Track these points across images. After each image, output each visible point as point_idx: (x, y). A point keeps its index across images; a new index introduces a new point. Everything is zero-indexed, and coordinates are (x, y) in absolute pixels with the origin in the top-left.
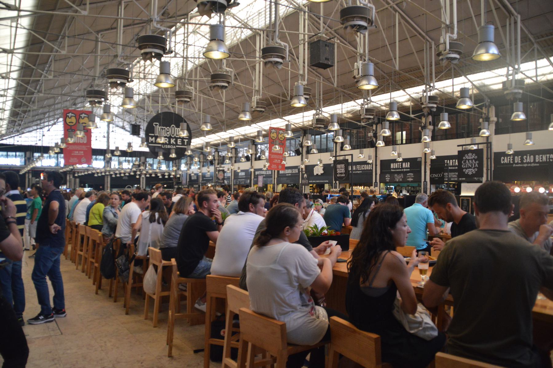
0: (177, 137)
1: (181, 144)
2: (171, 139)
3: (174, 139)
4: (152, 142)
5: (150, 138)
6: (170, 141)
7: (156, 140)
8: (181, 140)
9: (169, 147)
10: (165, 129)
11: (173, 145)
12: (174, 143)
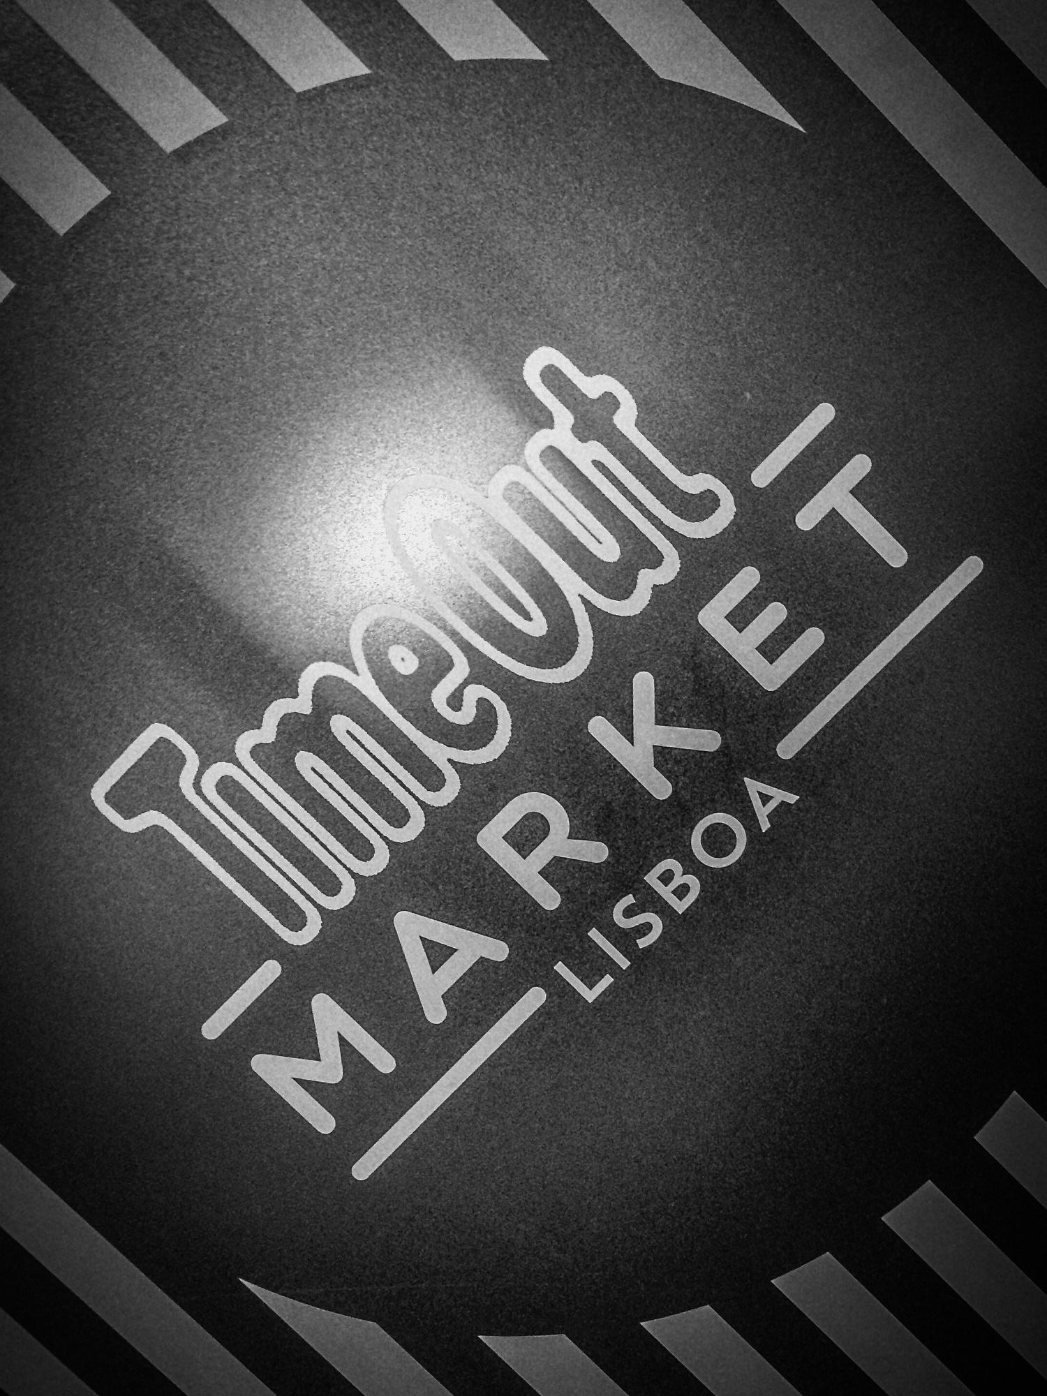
0: (635, 604)
1: (812, 640)
2: (600, 728)
3: (644, 685)
8: (747, 579)
12: (707, 740)
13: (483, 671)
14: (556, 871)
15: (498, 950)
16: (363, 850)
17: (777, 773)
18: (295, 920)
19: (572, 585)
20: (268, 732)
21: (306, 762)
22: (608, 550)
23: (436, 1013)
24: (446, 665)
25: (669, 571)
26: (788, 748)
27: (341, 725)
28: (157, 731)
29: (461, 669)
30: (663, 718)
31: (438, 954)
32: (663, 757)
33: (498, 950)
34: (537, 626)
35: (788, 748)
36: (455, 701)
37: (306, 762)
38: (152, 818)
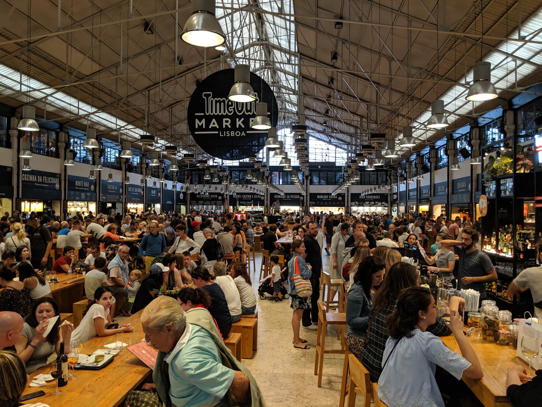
0: (247, 114)
2: (237, 119)
3: (243, 119)
4: (200, 128)
5: (197, 121)
6: (233, 123)
7: (207, 124)
9: (233, 134)
10: (224, 101)
11: (240, 128)
12: (243, 126)
13: (234, 109)
14: (226, 126)
15: (218, 127)
16: (216, 112)
17: (245, 133)
18: (208, 113)
19: (244, 109)
20: (217, 100)
21: (218, 104)
22: (249, 109)
23: (210, 127)
24: (232, 106)
25: (251, 114)
26: (248, 132)
27: (222, 103)
28: (211, 93)
29: (233, 107)
30: (242, 122)
31: (214, 124)
32: (240, 125)
33: (218, 127)
34: (240, 109)
35: (248, 132)
36: (231, 109)
37: (218, 104)
38: (205, 98)
